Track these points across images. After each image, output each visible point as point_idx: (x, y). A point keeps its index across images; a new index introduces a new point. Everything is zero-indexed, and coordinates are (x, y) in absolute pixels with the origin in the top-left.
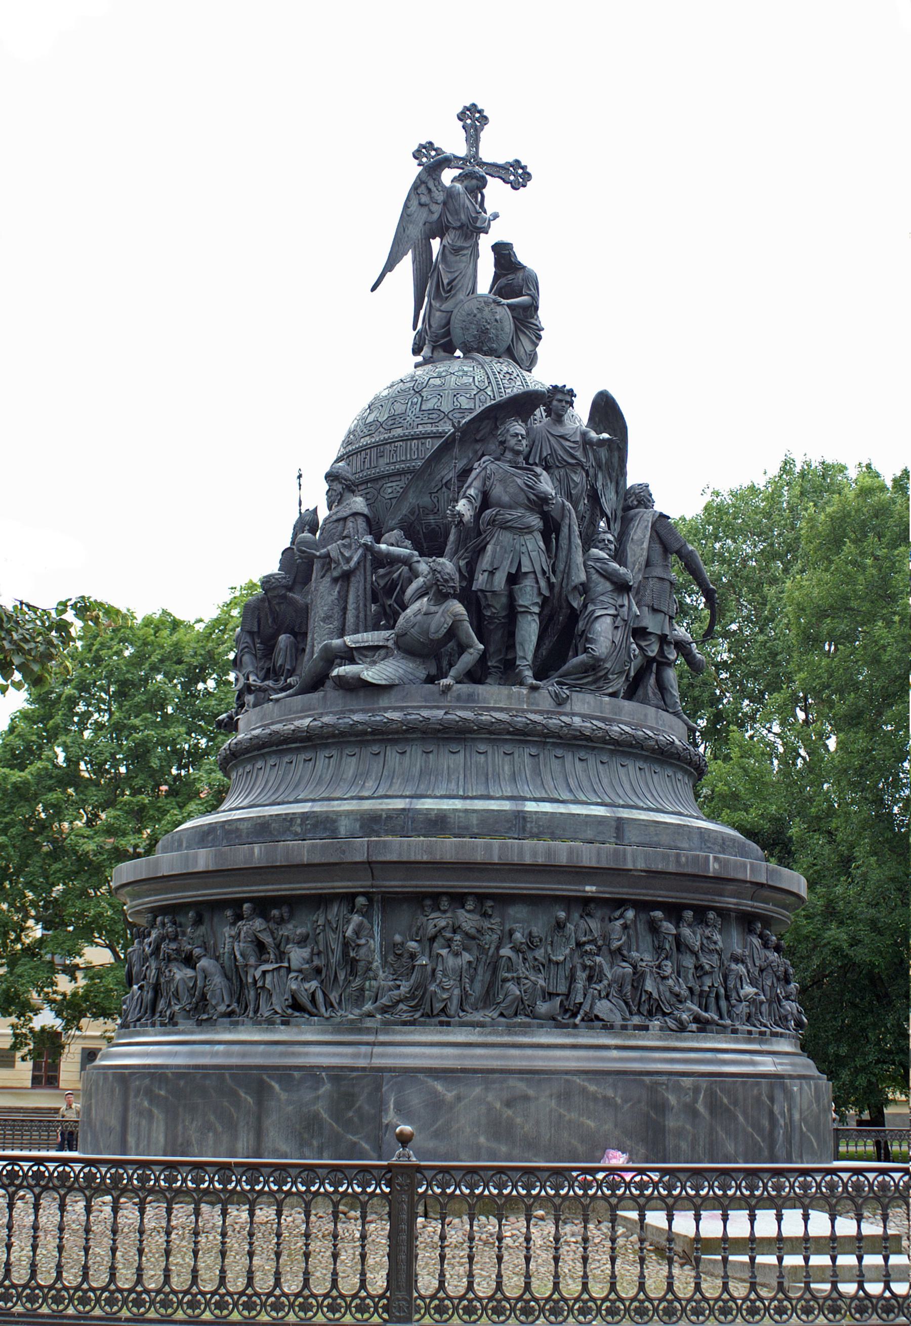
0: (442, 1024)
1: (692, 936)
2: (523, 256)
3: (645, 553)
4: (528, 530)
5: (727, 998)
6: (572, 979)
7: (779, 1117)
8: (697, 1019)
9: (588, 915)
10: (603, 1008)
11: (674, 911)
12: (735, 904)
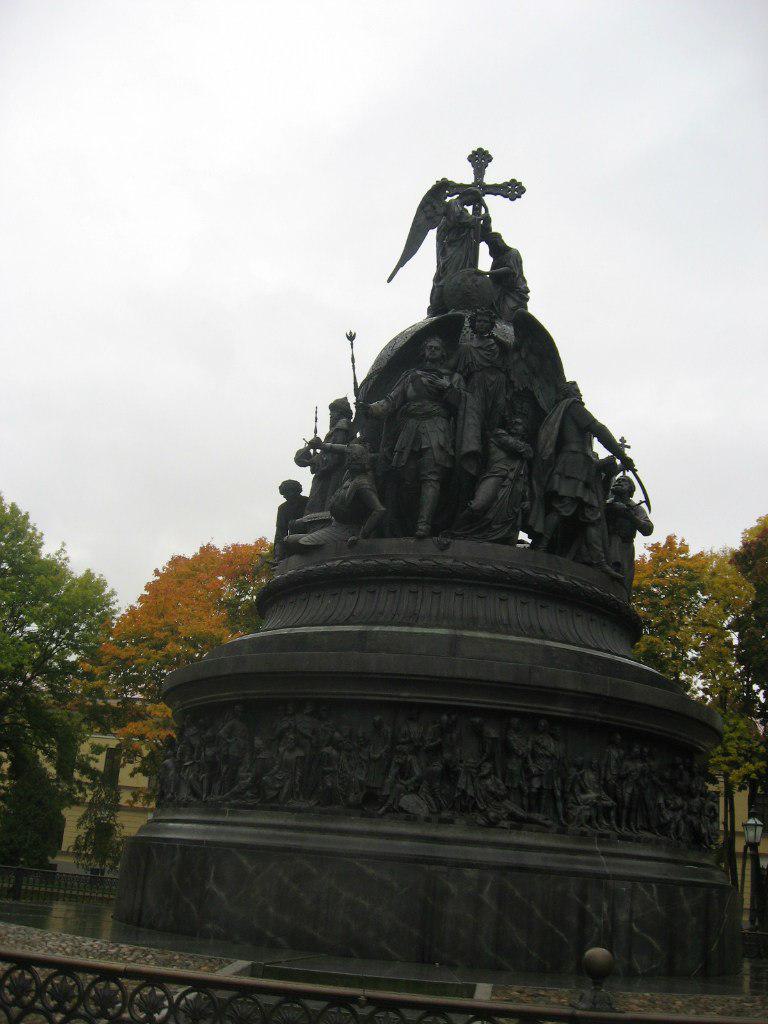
0: (273, 809)
1: (520, 743)
2: (509, 241)
3: (556, 432)
4: (428, 415)
5: (565, 801)
6: (386, 774)
7: (594, 914)
8: (512, 816)
9: (411, 719)
10: (408, 801)
11: (502, 716)
12: (572, 713)
